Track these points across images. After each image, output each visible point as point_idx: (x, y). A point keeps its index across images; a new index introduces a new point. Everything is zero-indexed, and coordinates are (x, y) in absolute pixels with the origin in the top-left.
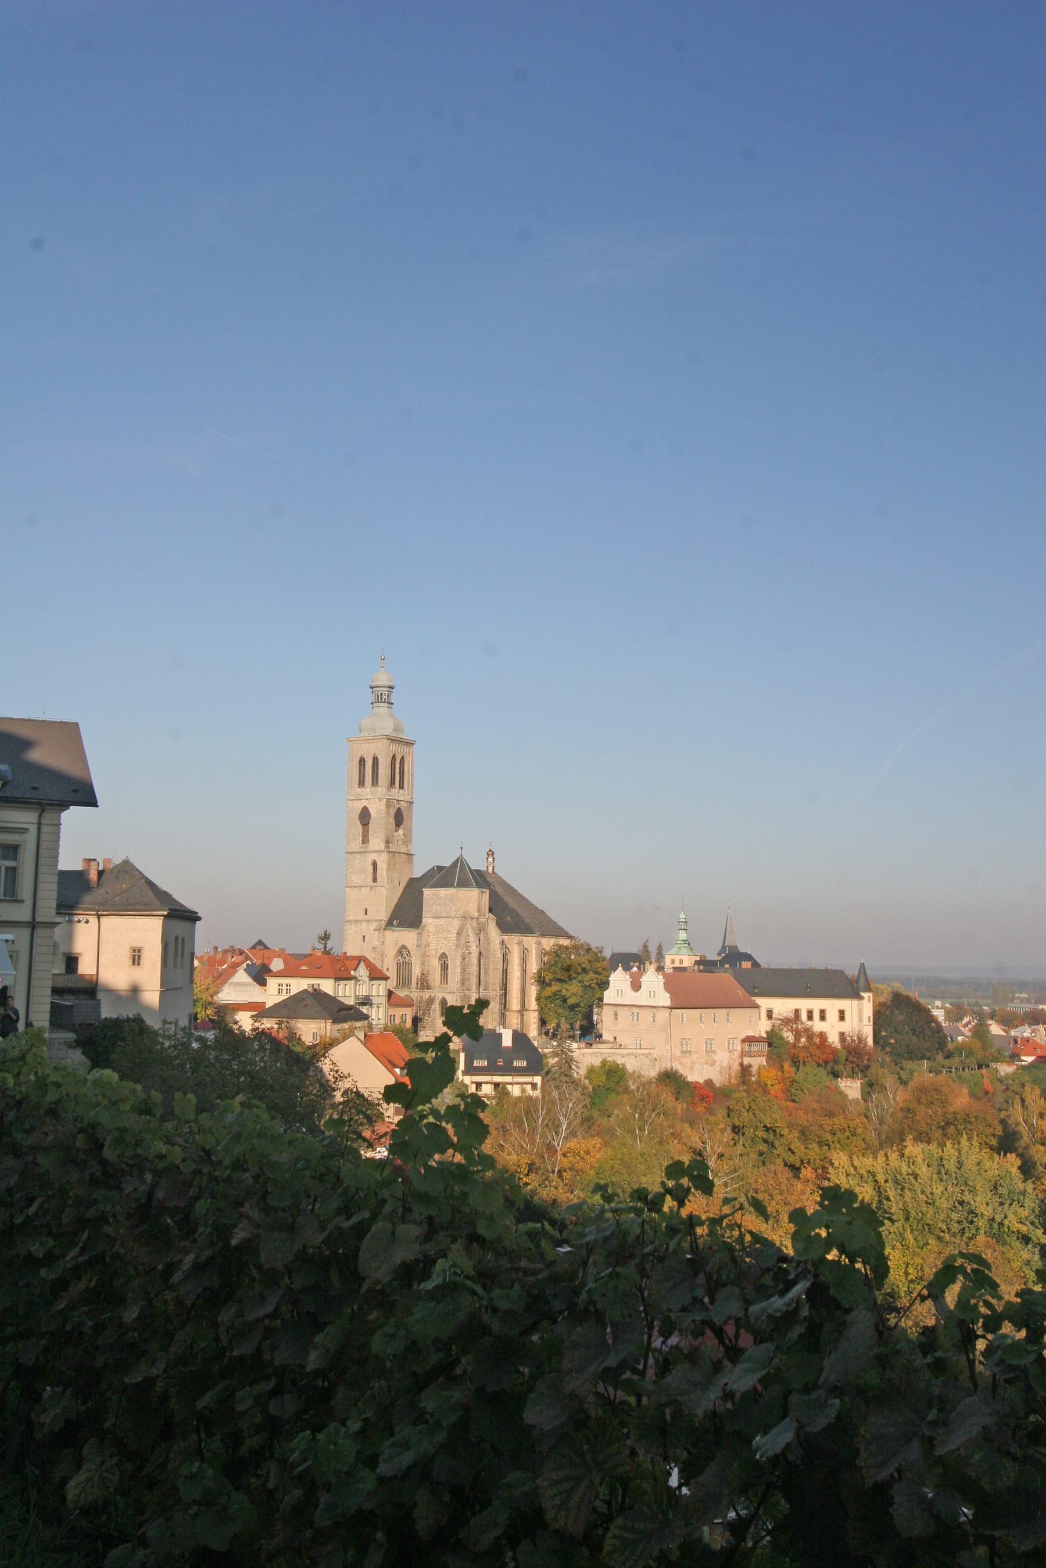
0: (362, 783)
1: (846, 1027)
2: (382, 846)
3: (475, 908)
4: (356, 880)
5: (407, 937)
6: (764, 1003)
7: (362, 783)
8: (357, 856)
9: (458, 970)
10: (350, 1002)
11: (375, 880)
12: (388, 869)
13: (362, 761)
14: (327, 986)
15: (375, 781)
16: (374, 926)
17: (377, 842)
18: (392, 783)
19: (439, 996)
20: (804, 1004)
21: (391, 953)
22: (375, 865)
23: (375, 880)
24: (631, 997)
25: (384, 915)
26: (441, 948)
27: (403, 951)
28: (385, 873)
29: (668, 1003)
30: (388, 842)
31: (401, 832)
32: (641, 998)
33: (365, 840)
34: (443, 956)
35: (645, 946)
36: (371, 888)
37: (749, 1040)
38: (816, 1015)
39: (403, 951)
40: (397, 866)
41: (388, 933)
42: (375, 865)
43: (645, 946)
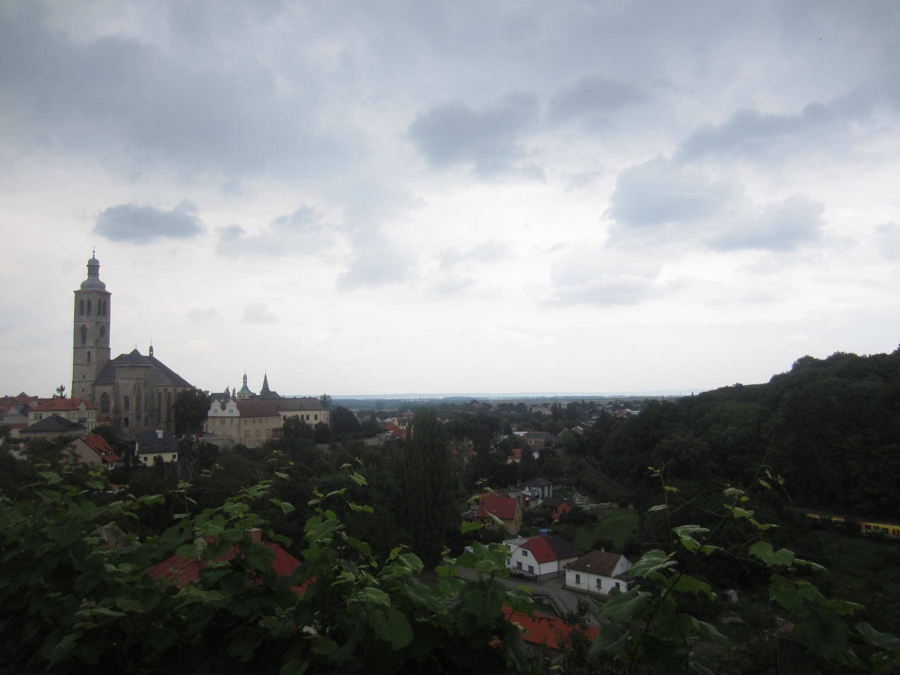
1: (317, 422)
2: (93, 345)
5: (108, 389)
6: (282, 413)
9: (134, 404)
10: (75, 421)
11: (89, 361)
14: (63, 415)
16: (88, 384)
17: (90, 343)
18: (99, 313)
20: (300, 413)
21: (98, 397)
22: (89, 353)
23: (89, 361)
24: (221, 413)
25: (93, 378)
27: (104, 395)
29: (238, 415)
30: (96, 342)
32: (226, 413)
34: (126, 398)
35: (227, 390)
37: (275, 430)
38: (305, 418)
39: (104, 395)
41: (96, 387)
42: (89, 353)
43: (227, 390)
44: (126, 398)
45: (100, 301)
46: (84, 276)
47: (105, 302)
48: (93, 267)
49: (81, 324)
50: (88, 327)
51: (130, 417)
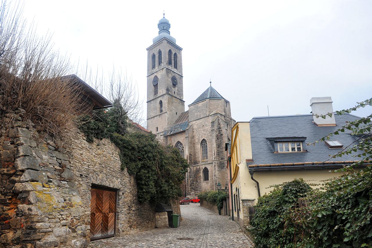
0: (154, 67)
3: (222, 110)
4: (153, 115)
7: (154, 67)
8: (152, 102)
9: (215, 145)
11: (161, 111)
12: (169, 103)
13: (154, 56)
15: (160, 63)
17: (162, 91)
19: (203, 167)
22: (161, 102)
26: (202, 137)
28: (167, 105)
31: (176, 88)
33: (156, 92)
34: (204, 142)
36: (160, 115)
40: (174, 104)
44: (204, 142)
45: (170, 51)
46: (155, 33)
47: (175, 54)
48: (164, 26)
49: (153, 76)
50: (159, 77)
51: (209, 167)
